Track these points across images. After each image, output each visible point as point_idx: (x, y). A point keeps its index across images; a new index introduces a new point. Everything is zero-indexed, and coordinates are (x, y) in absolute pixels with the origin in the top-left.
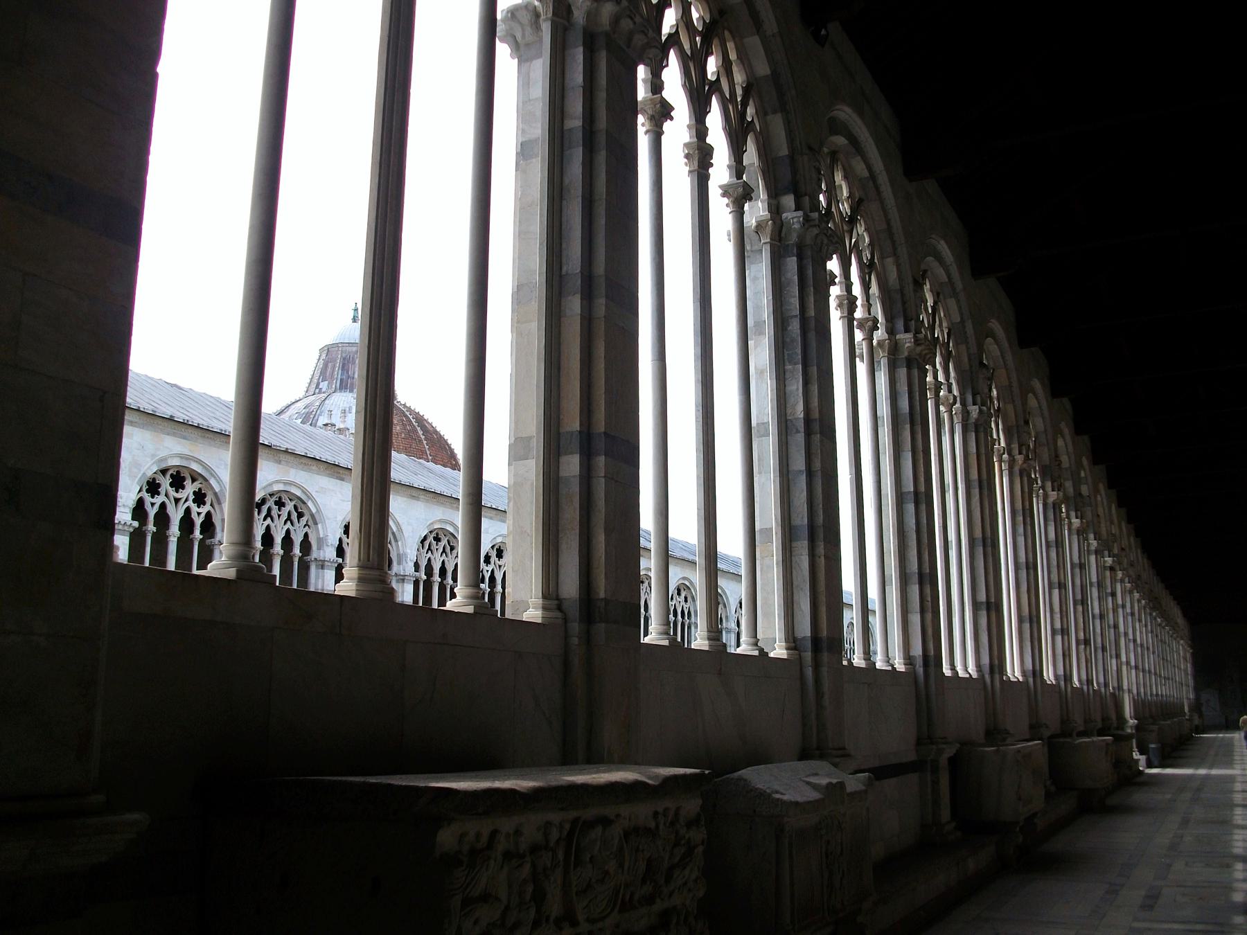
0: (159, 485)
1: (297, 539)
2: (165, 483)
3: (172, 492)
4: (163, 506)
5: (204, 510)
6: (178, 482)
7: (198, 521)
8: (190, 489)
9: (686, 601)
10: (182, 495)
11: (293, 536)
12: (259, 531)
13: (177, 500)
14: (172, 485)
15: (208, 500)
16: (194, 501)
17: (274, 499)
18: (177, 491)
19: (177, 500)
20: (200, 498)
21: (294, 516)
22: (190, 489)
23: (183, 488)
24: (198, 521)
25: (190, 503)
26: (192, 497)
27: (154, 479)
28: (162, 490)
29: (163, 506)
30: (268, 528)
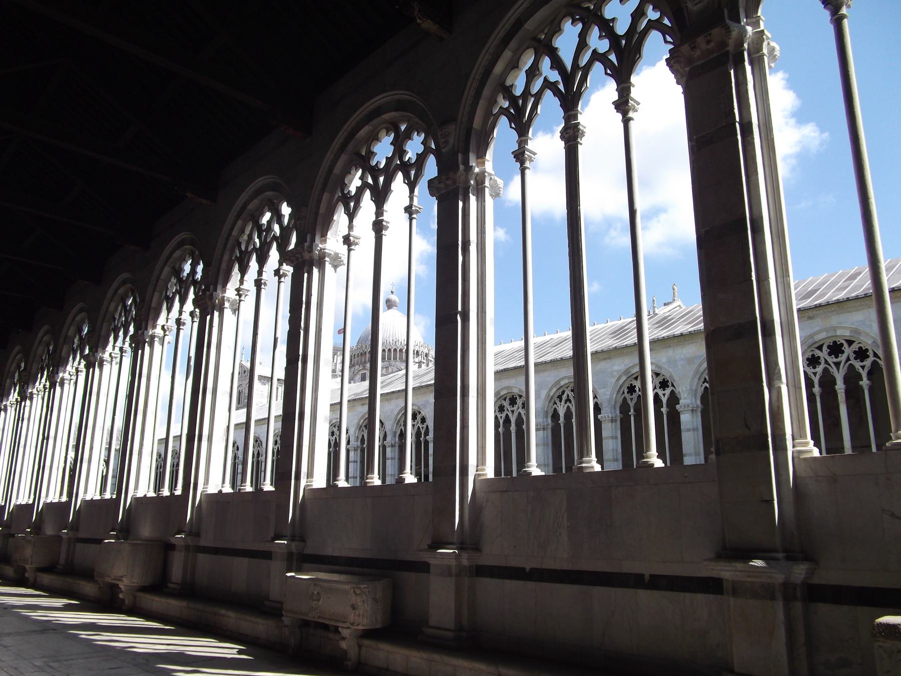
0: (819, 357)
2: (823, 354)
3: (831, 360)
5: (868, 363)
8: (848, 351)
10: (842, 358)
13: (837, 365)
14: (830, 354)
15: (870, 353)
16: (856, 359)
23: (843, 352)
26: (852, 356)
27: (813, 355)
28: (823, 361)
29: (826, 371)
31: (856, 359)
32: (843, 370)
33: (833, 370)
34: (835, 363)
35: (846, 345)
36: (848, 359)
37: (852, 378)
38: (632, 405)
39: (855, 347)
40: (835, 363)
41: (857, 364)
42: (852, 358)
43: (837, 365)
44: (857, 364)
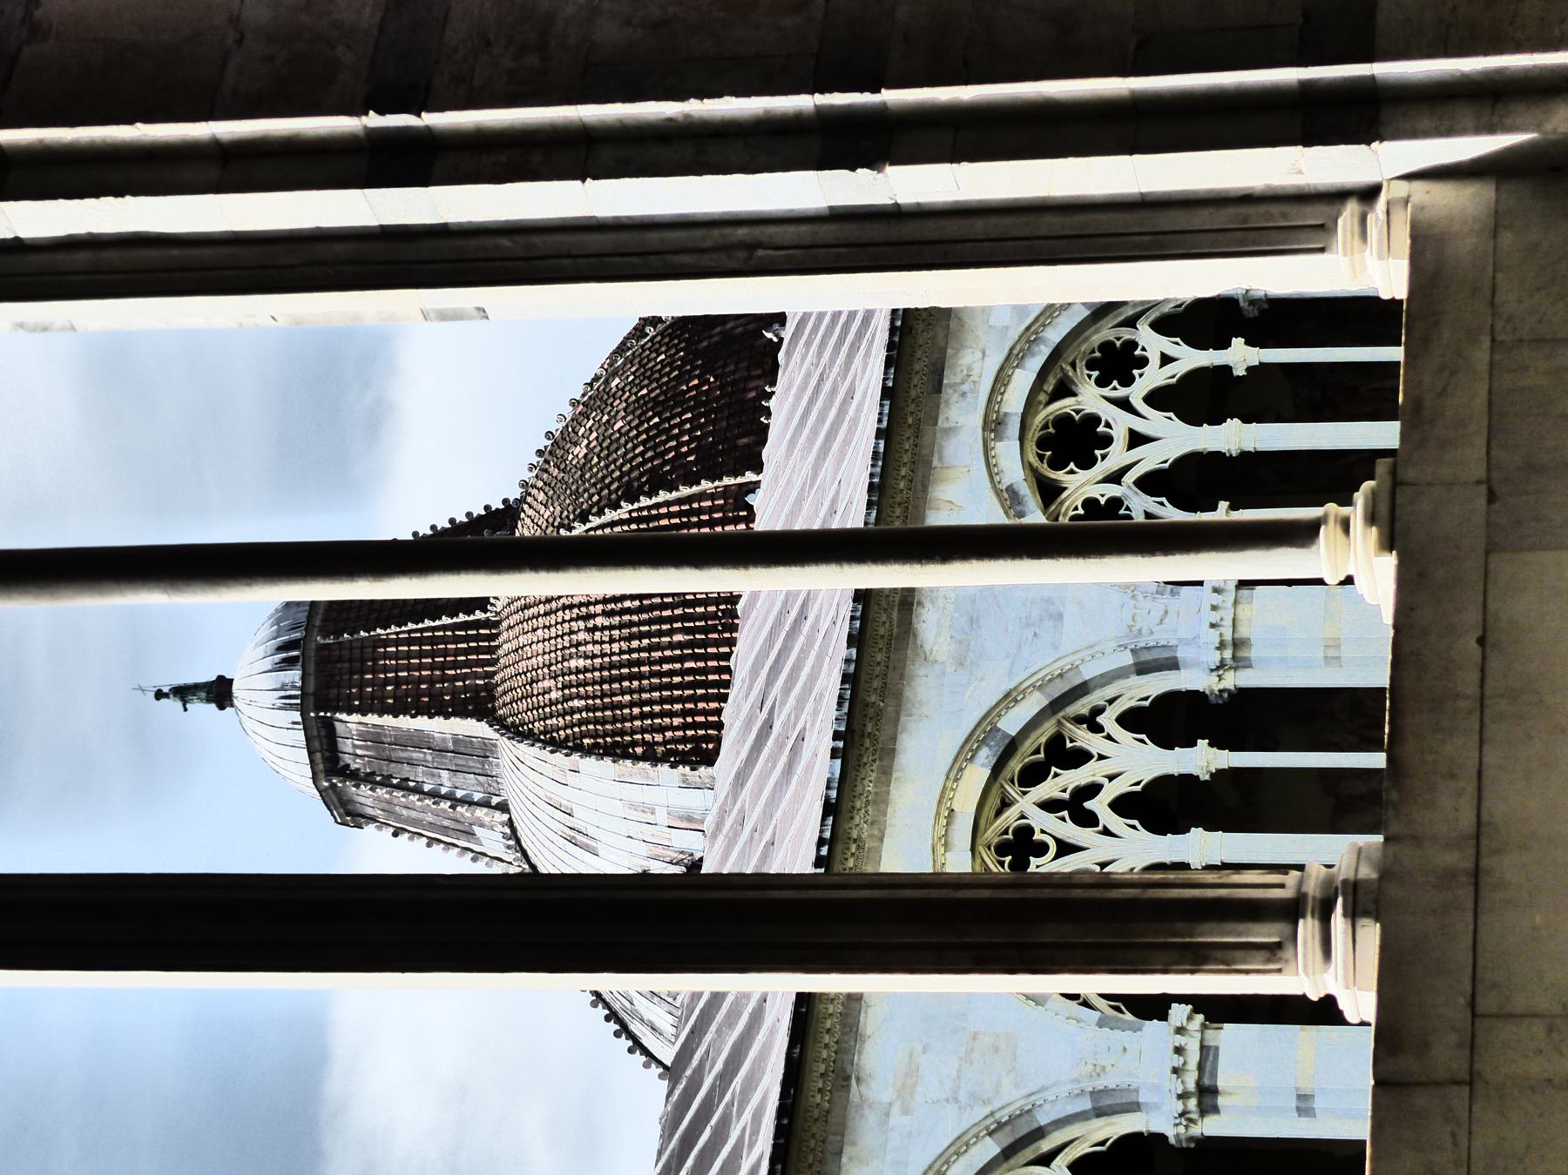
4: (1149, 484)
5: (1151, 342)
6: (1075, 441)
8: (1090, 398)
13: (1136, 439)
14: (1087, 463)
18: (1107, 441)
20: (1118, 364)
22: (1090, 398)
25: (1136, 393)
26: (1122, 392)
29: (1149, 484)
31: (1128, 381)
33: (1151, 458)
34: (1131, 446)
35: (1065, 405)
36: (1124, 404)
37: (1196, 398)
38: (1191, 359)
40: (1131, 446)
41: (1152, 377)
43: (1136, 439)
44: (1152, 377)
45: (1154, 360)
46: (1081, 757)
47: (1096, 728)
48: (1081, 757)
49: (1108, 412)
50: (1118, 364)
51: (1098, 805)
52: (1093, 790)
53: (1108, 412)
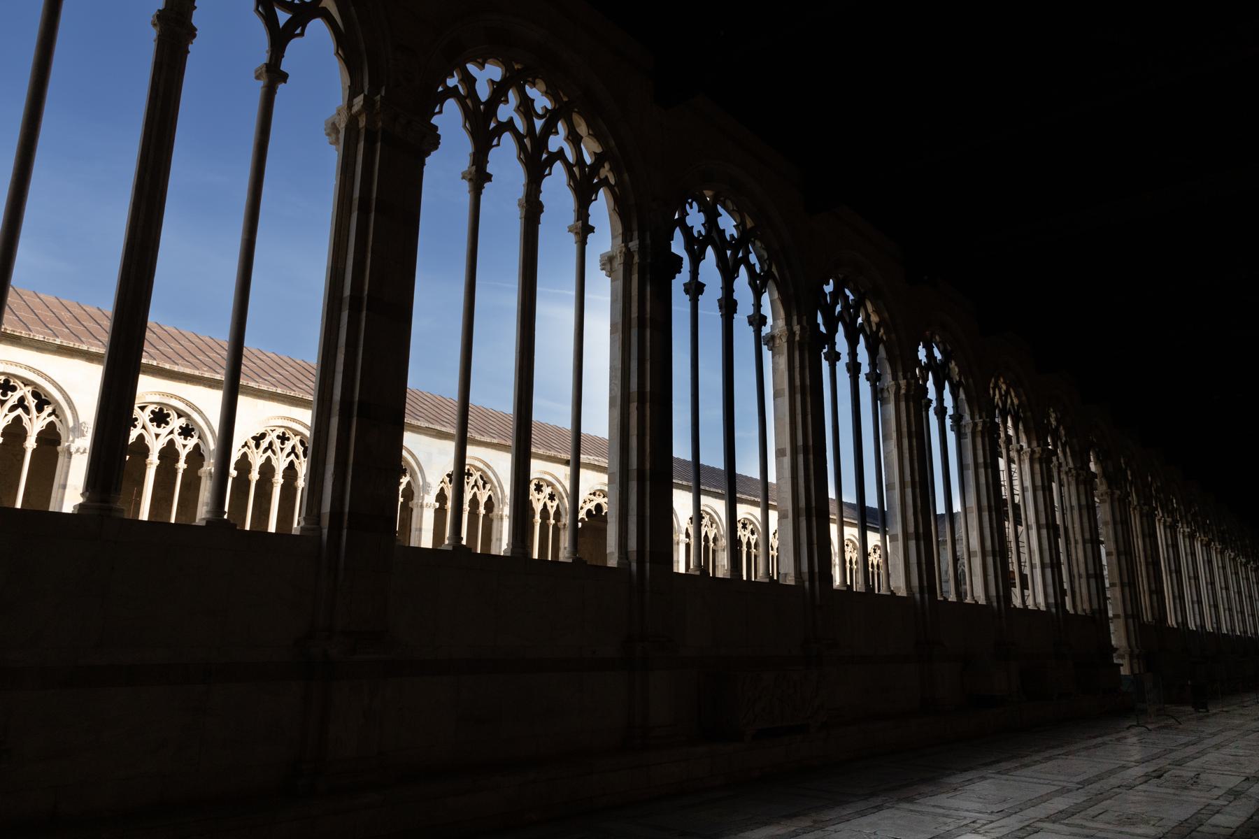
1: (483, 499)
3: (153, 428)
7: (552, 512)
8: (176, 423)
9: (753, 533)
11: (479, 497)
12: (468, 497)
13: (157, 436)
17: (276, 433)
19: (157, 436)
20: (186, 432)
21: (480, 483)
22: (176, 423)
24: (552, 512)
26: (176, 432)
30: (475, 495)
32: (162, 442)
33: (149, 440)
36: (171, 432)
39: (183, 422)
41: (179, 441)
42: (176, 432)
44: (179, 441)
45: (185, 442)
46: (40, 409)
47: (49, 415)
48: (40, 409)
49: (169, 428)
50: (186, 432)
51: (20, 411)
52: (273, 452)
53: (169, 428)
